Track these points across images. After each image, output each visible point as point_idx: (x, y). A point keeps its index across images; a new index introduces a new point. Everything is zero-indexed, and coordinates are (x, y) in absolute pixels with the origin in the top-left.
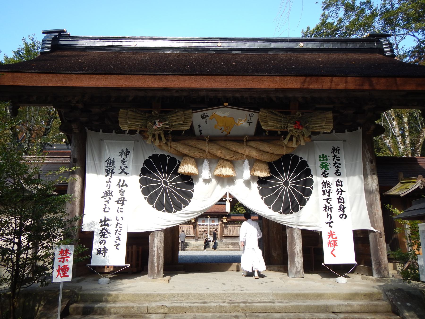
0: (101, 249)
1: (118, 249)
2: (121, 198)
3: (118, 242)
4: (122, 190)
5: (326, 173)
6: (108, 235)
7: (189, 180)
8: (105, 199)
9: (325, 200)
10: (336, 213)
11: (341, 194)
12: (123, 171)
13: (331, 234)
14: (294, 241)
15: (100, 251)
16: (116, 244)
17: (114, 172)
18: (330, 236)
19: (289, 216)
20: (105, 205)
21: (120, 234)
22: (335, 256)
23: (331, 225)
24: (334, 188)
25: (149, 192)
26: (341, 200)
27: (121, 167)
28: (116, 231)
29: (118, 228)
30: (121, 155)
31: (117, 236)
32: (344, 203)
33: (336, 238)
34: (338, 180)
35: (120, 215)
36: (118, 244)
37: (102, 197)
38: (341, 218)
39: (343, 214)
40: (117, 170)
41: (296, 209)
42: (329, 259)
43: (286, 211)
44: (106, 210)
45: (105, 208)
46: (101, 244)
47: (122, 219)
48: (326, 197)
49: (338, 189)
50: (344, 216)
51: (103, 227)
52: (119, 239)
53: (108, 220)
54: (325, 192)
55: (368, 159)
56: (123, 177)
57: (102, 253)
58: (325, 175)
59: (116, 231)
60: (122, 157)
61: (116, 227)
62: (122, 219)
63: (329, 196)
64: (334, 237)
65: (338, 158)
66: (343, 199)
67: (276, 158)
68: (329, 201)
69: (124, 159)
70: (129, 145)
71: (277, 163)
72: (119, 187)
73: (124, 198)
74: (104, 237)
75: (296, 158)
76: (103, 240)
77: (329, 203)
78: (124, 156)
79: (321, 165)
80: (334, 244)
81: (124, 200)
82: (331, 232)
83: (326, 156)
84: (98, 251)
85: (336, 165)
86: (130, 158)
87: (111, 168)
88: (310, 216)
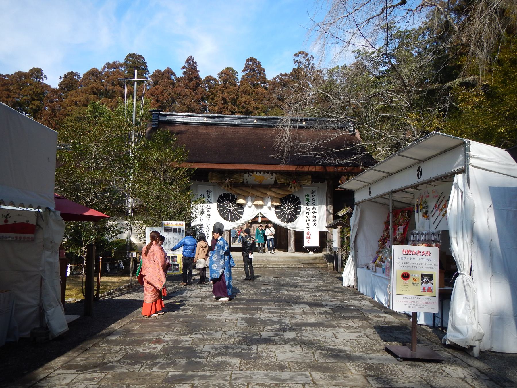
7: (241, 206)
10: (311, 223)
13: (308, 233)
19: (289, 224)
25: (222, 211)
26: (314, 217)
35: (208, 223)
41: (292, 221)
42: (306, 244)
43: (288, 222)
54: (307, 213)
56: (209, 204)
67: (284, 196)
70: (211, 188)
71: (285, 198)
75: (294, 196)
80: (309, 237)
86: (212, 195)
88: (300, 224)
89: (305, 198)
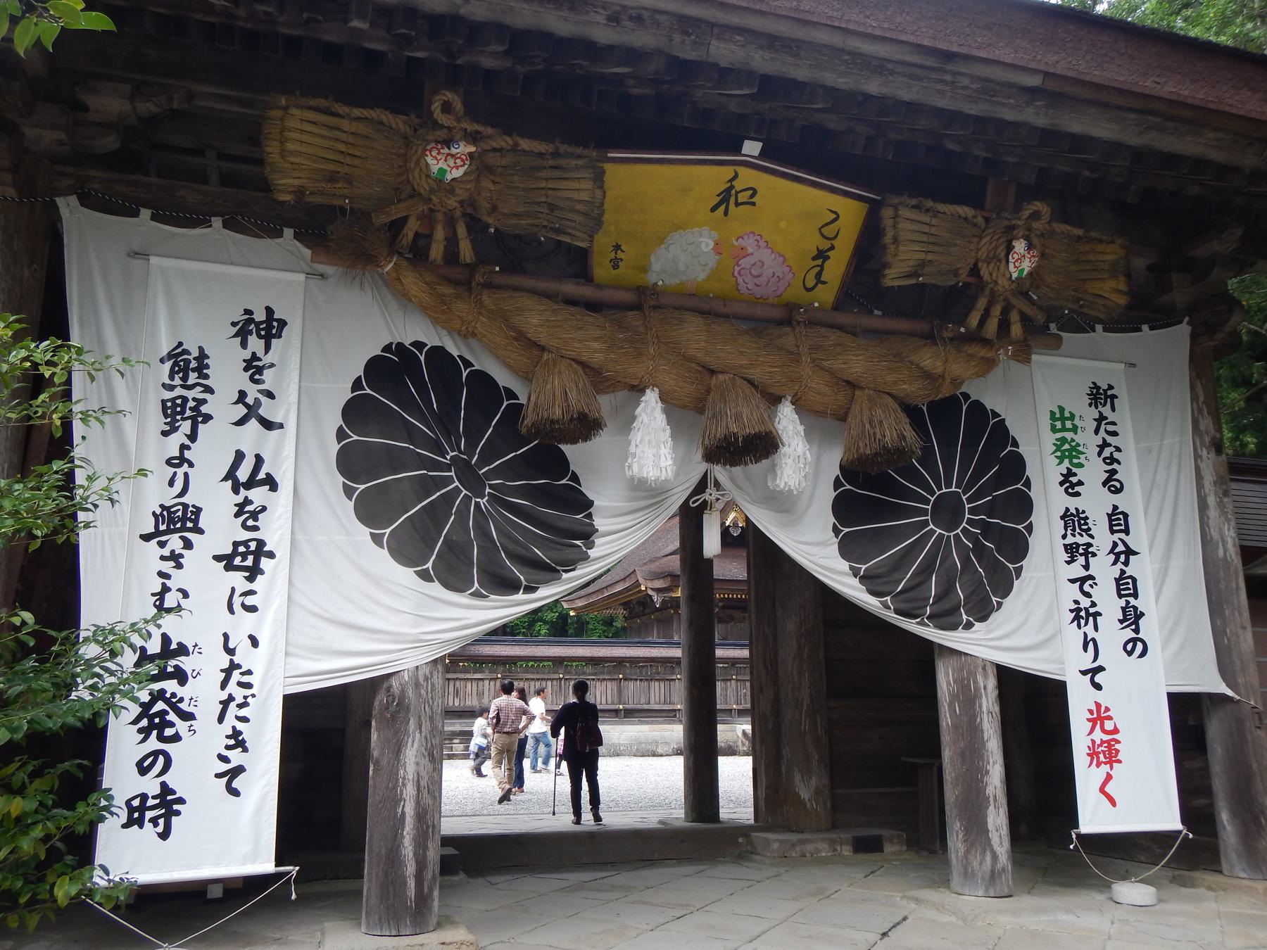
0: (144, 797)
1: (235, 793)
2: (245, 543)
3: (236, 757)
4: (247, 501)
5: (1074, 480)
6: (181, 726)
8: (162, 545)
9: (1073, 581)
10: (1111, 634)
11: (1126, 563)
12: (252, 412)
13: (1099, 717)
14: (983, 744)
15: (143, 808)
16: (224, 767)
17: (207, 418)
18: (1093, 721)
20: (162, 574)
21: (244, 720)
22: (1113, 802)
23: (1098, 679)
24: (1103, 539)
26: (1126, 586)
27: (242, 395)
28: (225, 704)
29: (232, 687)
30: (242, 334)
31: (227, 729)
32: (1135, 595)
33: (1116, 731)
34: (1115, 507)
35: (242, 625)
36: (239, 770)
37: (146, 538)
38: (1130, 653)
39: (1134, 641)
40: (222, 407)
44: (170, 600)
45: (166, 589)
46: (143, 770)
47: (254, 642)
48: (1077, 570)
49: (1115, 545)
50: (1140, 646)
51: (156, 686)
52: (237, 741)
53: (183, 650)
54: (1071, 550)
55: (1207, 439)
56: (250, 438)
57: (154, 821)
58: (1073, 486)
59: (225, 704)
60: (244, 345)
61: (224, 685)
62: (254, 642)
63: (1087, 567)
64: (1109, 725)
65: (1110, 428)
66: (1134, 580)
68: (1086, 588)
69: (254, 357)
72: (236, 490)
73: (261, 543)
74: (161, 738)
76: (156, 754)
77: (1088, 595)
78: (255, 344)
79: (1058, 448)
80: (1107, 754)
81: (261, 551)
82: (1098, 705)
83: (1072, 417)
84: (131, 810)
85: (1107, 452)
87: (190, 394)
89: (1049, 439)
